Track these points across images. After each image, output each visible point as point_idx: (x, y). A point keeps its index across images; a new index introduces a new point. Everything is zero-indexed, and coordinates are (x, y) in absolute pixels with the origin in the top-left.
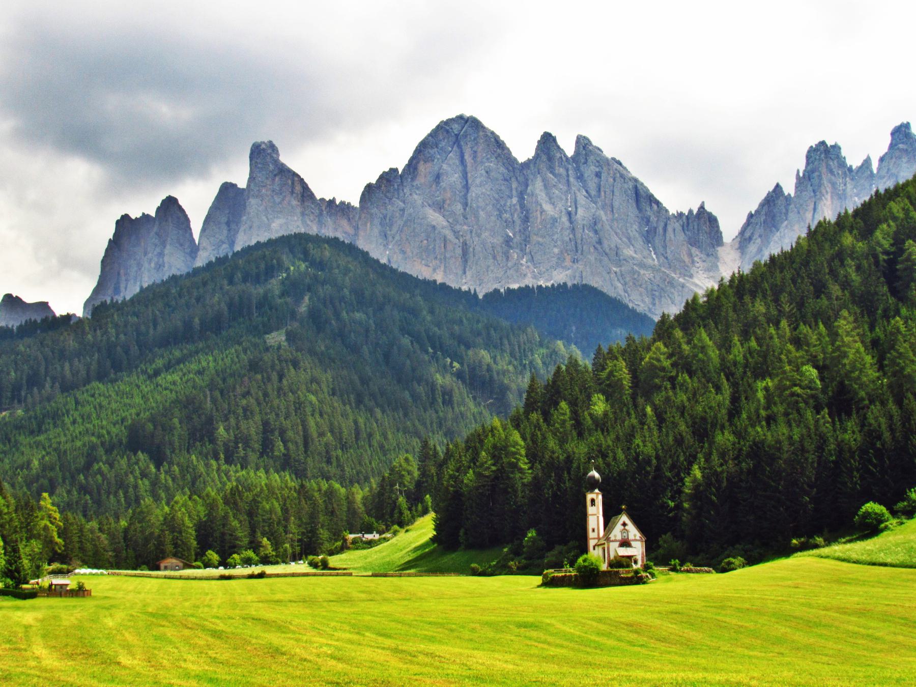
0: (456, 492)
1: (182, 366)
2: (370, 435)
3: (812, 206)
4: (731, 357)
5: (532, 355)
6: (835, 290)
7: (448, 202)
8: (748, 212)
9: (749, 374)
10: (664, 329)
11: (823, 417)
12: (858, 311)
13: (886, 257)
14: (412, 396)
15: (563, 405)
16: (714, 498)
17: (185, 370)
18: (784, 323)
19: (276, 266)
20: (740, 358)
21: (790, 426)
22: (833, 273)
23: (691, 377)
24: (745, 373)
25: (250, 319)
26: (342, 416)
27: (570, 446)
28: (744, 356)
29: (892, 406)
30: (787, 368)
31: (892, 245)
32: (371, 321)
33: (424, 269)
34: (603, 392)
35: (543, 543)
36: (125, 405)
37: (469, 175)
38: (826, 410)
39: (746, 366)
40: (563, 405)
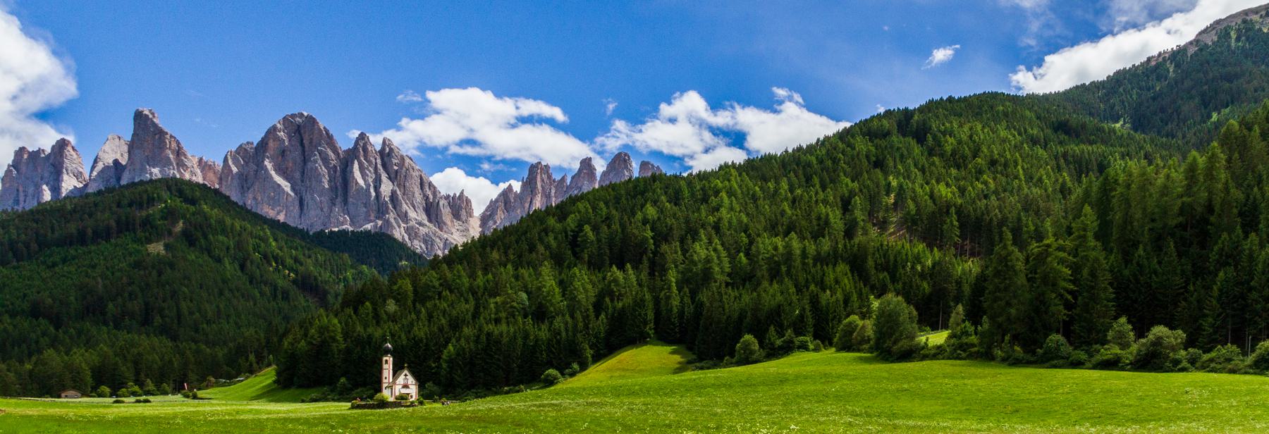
0: (293, 353)
1: (77, 261)
2: (228, 316)
3: (529, 200)
4: (476, 283)
5: (346, 273)
6: (541, 249)
7: (290, 169)
8: (490, 200)
9: (486, 294)
10: (435, 263)
11: (528, 321)
12: (553, 262)
13: (572, 234)
14: (260, 293)
15: (367, 303)
16: (461, 363)
17: (79, 264)
18: (509, 266)
19: (157, 199)
20: (481, 284)
21: (508, 325)
22: (541, 240)
23: (450, 293)
24: (484, 293)
25: (135, 233)
26: (207, 301)
27: (370, 330)
28: (484, 283)
29: (568, 318)
30: (510, 292)
31: (576, 227)
32: (231, 243)
33: (271, 211)
34: (394, 298)
35: (350, 386)
36: (26, 285)
37: (306, 154)
38: (530, 317)
39: (485, 289)
40: (367, 303)
